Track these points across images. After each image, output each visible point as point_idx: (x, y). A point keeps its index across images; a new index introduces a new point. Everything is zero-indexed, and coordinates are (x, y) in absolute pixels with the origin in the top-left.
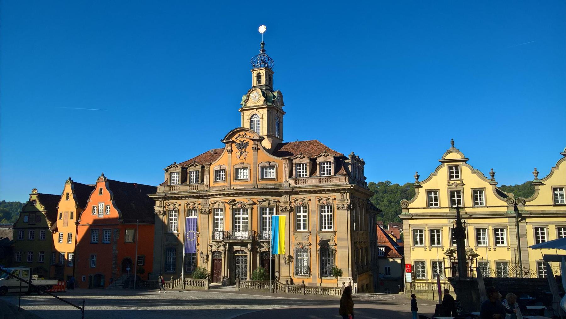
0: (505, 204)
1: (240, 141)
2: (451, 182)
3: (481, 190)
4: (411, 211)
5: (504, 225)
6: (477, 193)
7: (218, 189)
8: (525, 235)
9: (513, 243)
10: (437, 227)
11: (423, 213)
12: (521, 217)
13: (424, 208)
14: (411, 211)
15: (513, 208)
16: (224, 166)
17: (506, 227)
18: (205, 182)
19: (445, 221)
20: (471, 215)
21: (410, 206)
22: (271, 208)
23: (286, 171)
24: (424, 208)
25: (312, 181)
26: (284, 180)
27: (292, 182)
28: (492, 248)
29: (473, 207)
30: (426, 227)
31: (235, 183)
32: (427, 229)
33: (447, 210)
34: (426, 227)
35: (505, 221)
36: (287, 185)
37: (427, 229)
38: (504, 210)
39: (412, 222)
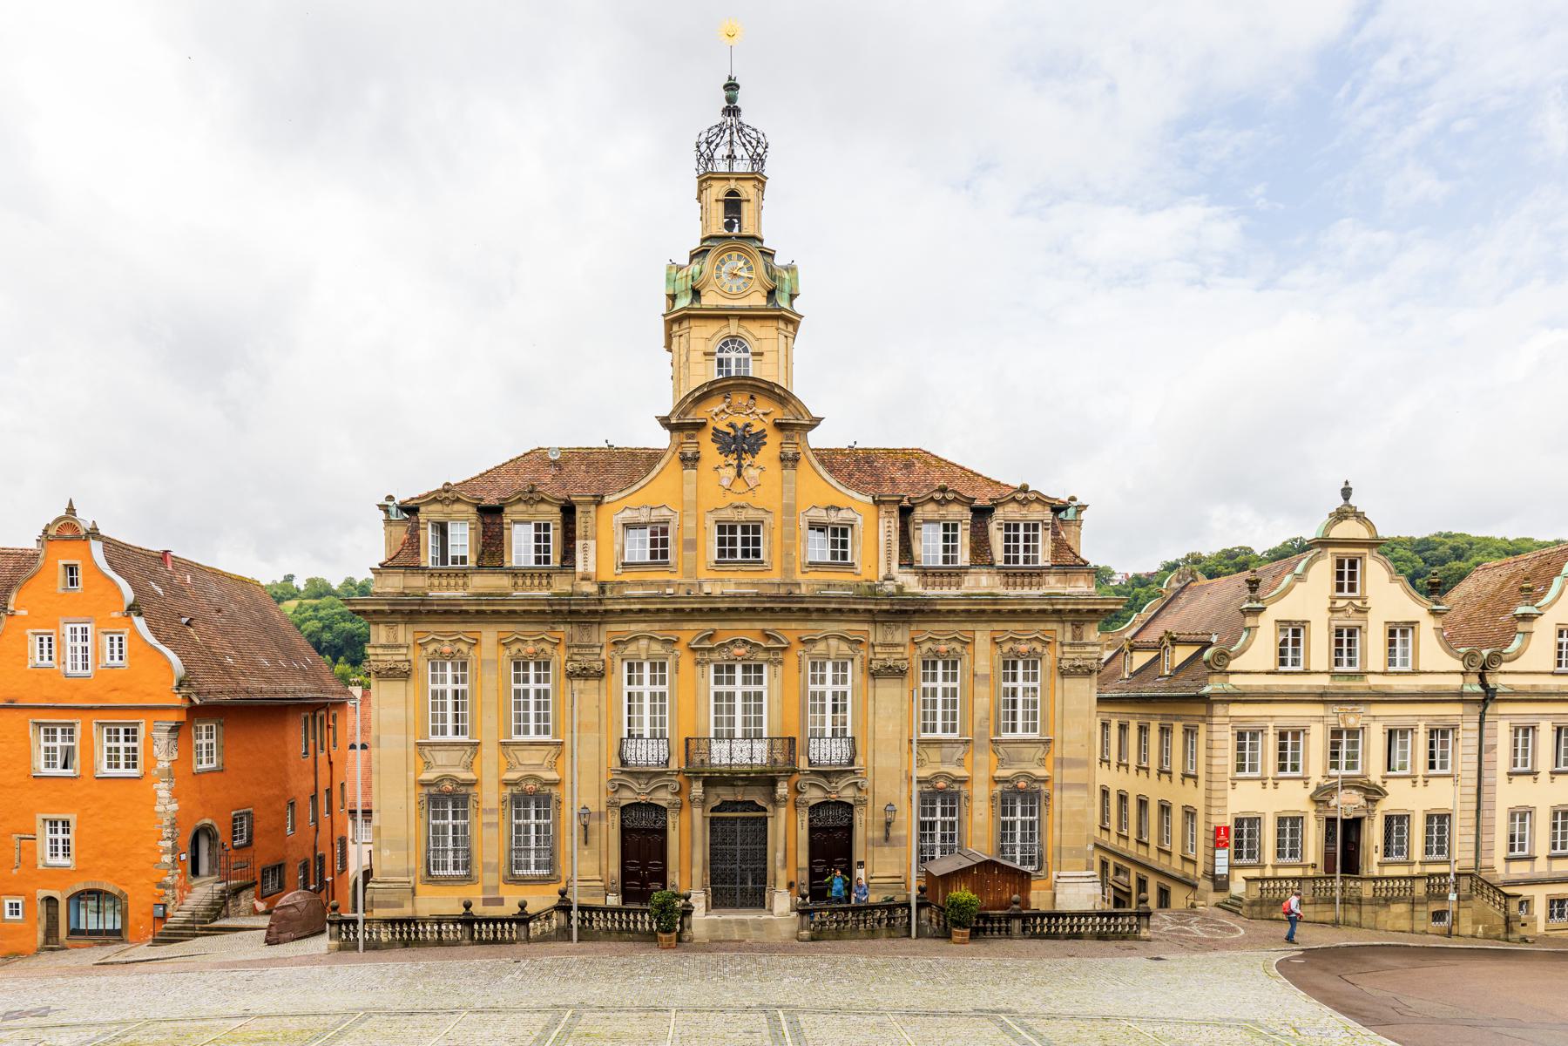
0: (1459, 666)
2: (1340, 604)
3: (1408, 627)
5: (1451, 721)
6: (1397, 632)
7: (639, 592)
8: (1494, 746)
9: (1465, 766)
10: (1299, 723)
11: (1266, 686)
12: (1489, 696)
14: (1235, 680)
15: (1476, 679)
17: (1454, 728)
18: (580, 568)
19: (1319, 710)
20: (1387, 694)
22: (840, 666)
24: (1268, 673)
26: (883, 572)
28: (1420, 780)
30: (1271, 725)
32: (1271, 731)
33: (1325, 681)
34: (1271, 725)
35: (1457, 709)
36: (890, 587)
37: (1271, 731)
38: (1455, 682)
39: (1236, 710)
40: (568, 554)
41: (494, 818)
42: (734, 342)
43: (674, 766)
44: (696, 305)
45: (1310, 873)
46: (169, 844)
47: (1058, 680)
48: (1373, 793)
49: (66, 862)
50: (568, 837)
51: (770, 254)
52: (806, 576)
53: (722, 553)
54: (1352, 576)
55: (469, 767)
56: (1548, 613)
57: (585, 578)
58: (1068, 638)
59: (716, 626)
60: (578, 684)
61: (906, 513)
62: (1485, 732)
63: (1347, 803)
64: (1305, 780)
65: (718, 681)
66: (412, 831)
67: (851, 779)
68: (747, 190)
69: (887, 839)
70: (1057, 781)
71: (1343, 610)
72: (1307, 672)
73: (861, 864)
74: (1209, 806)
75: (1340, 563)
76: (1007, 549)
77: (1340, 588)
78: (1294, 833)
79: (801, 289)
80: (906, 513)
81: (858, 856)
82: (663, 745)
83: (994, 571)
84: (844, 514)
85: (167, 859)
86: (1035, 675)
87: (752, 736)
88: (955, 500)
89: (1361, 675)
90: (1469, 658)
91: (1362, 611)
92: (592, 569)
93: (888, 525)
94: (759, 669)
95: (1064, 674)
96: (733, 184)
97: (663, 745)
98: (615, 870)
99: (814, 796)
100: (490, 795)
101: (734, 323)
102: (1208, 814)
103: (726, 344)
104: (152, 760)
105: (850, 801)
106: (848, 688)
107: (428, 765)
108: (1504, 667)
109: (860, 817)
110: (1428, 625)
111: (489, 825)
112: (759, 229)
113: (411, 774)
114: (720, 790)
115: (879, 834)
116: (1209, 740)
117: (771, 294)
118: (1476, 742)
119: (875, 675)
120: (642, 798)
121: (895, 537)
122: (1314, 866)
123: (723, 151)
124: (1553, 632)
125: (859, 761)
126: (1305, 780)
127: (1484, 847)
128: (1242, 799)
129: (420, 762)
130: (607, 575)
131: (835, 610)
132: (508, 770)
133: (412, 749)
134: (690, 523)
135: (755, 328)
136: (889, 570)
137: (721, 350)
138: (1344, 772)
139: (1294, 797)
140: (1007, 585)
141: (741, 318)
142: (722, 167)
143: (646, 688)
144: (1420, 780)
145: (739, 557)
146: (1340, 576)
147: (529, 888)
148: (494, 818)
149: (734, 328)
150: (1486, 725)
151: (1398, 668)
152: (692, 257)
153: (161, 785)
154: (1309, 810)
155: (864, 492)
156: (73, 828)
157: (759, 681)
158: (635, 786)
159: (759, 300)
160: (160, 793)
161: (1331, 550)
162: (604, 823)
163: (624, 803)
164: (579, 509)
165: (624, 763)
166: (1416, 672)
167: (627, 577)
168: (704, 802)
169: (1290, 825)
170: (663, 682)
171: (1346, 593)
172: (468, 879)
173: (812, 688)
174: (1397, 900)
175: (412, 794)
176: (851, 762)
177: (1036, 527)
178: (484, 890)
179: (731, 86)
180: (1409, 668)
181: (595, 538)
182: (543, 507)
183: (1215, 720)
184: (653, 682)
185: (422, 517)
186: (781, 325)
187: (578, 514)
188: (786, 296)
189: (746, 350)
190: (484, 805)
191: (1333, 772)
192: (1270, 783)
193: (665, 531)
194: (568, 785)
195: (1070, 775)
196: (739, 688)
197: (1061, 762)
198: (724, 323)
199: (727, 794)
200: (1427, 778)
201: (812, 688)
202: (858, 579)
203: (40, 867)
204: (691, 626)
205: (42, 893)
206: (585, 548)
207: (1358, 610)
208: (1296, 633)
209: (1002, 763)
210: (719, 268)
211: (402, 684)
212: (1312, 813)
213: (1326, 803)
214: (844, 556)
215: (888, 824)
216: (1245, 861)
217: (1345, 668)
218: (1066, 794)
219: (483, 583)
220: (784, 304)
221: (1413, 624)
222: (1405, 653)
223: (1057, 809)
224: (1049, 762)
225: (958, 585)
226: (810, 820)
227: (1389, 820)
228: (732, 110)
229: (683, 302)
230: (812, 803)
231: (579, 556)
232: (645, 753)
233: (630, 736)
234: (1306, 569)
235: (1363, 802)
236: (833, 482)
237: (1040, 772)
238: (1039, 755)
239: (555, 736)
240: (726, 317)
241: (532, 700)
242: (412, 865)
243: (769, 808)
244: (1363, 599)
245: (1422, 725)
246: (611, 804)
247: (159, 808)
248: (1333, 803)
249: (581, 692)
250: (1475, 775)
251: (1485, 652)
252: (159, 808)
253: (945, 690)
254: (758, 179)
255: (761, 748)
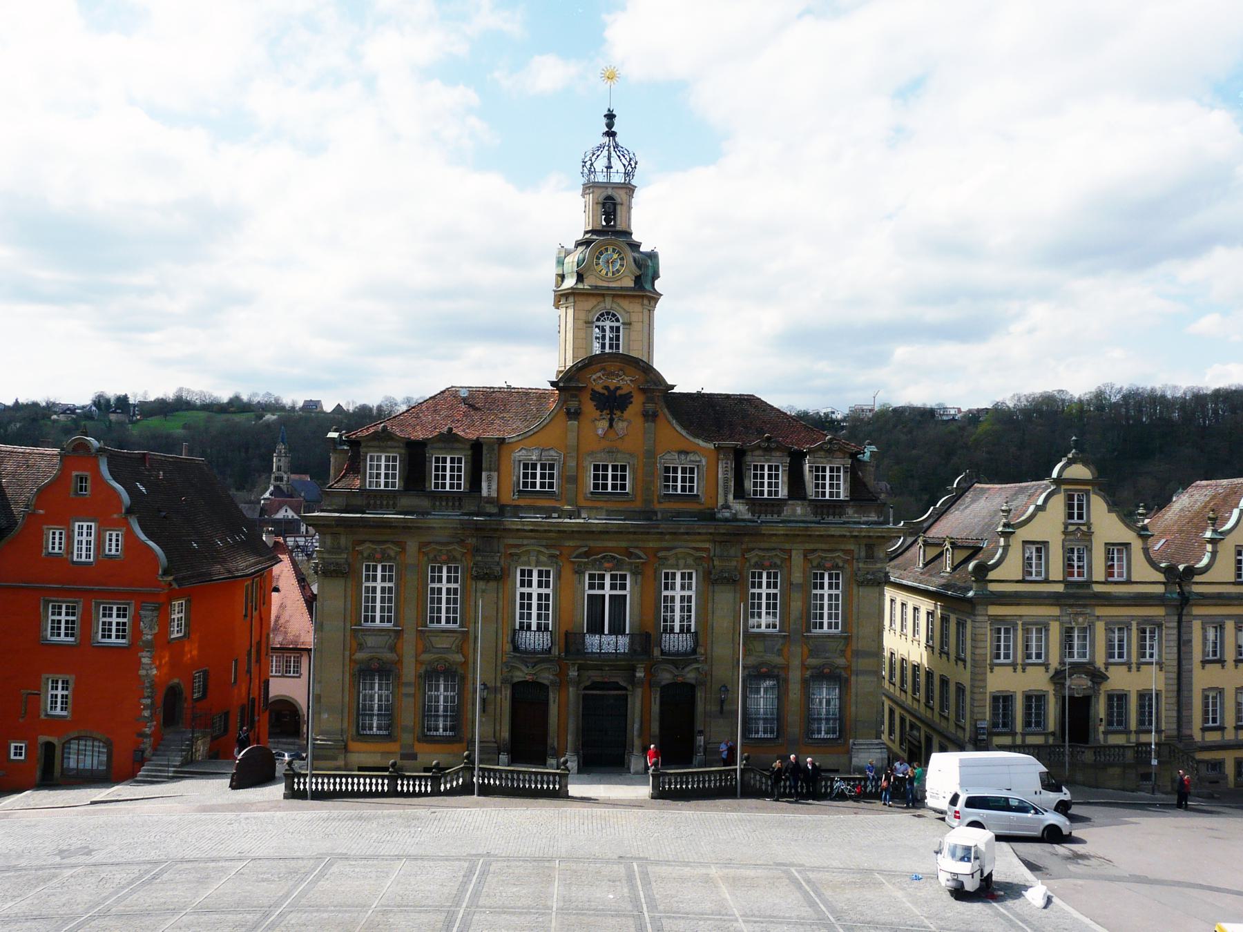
0: (1161, 577)
1: (606, 388)
2: (1071, 528)
4: (993, 587)
8: (1190, 641)
9: (1169, 657)
13: (1018, 582)
16: (552, 453)
17: (1160, 626)
18: (485, 493)
19: (1055, 611)
21: (992, 575)
23: (726, 480)
24: (1018, 582)
25: (794, 511)
26: (721, 502)
27: (740, 508)
28: (1134, 666)
29: (1106, 583)
30: (1020, 623)
31: (590, 504)
32: (1020, 627)
33: (1060, 588)
34: (1020, 623)
35: (1158, 612)
37: (1020, 627)
38: (1160, 589)
39: (994, 610)
40: (475, 483)
41: (411, 690)
42: (608, 313)
43: (555, 651)
44: (580, 286)
45: (1051, 741)
46: (148, 701)
47: (855, 587)
48: (1098, 677)
49: (64, 713)
50: (470, 707)
51: (635, 246)
52: (662, 506)
53: (596, 486)
54: (1080, 507)
55: (393, 649)
56: (1228, 538)
57: (489, 500)
58: (863, 554)
59: (591, 544)
60: (481, 585)
61: (739, 456)
62: (1183, 630)
63: (1078, 684)
64: (1046, 666)
65: (592, 587)
66: (347, 699)
67: (695, 666)
68: (620, 196)
69: (721, 711)
70: (854, 668)
71: (1073, 533)
72: (1047, 581)
73: (701, 732)
74: (973, 686)
75: (1071, 498)
76: (817, 486)
77: (1071, 516)
78: (1038, 707)
79: (661, 273)
80: (739, 456)
81: (699, 726)
82: (547, 636)
83: (806, 503)
84: (692, 457)
85: (146, 713)
86: (837, 584)
87: (617, 629)
88: (777, 449)
89: (1089, 583)
90: (1170, 571)
91: (1089, 535)
92: (494, 495)
93: (724, 471)
94: (623, 577)
95: (861, 584)
96: (610, 192)
97: (547, 636)
98: (506, 734)
99: (666, 677)
100: (409, 671)
101: (608, 301)
102: (972, 692)
103: (602, 315)
104: (137, 633)
105: (693, 682)
106: (692, 593)
107: (361, 647)
108: (1197, 579)
109: (699, 694)
110: (1137, 545)
111: (407, 695)
112: (629, 226)
113: (347, 653)
114: (591, 673)
115: (715, 708)
116: (974, 635)
117: (638, 279)
118: (1175, 637)
119: (714, 582)
120: (528, 678)
121: (731, 475)
122: (1053, 734)
123: (600, 164)
124: (1233, 551)
125: (701, 650)
126: (1046, 666)
127: (1184, 719)
128: (1000, 680)
129: (355, 645)
130: (509, 498)
131: (683, 534)
132: (424, 652)
133: (348, 633)
134: (572, 463)
135: (625, 304)
136: (726, 500)
137: (598, 320)
138: (1076, 659)
139: (1038, 680)
140: (815, 514)
141: (614, 296)
142: (601, 178)
143: (535, 590)
144: (1134, 666)
145: (610, 490)
146: (1071, 507)
147: (438, 747)
148: (411, 690)
149: (608, 304)
150: (1184, 624)
151: (1116, 578)
152: (576, 247)
153: (144, 654)
154: (1049, 688)
155: (706, 440)
156: (71, 686)
157: (623, 587)
158: (524, 668)
159: (629, 283)
160: (145, 660)
161: (1063, 487)
162: (499, 696)
163: (516, 680)
164: (485, 448)
165: (516, 648)
166: (1129, 582)
167: (522, 503)
168: (579, 683)
169: (1034, 701)
170: (547, 586)
171: (1076, 520)
172: (389, 738)
173: (665, 593)
174: (1112, 765)
175: (347, 668)
176: (694, 651)
177: (838, 470)
178: (401, 747)
179: (610, 117)
180: (1124, 578)
181: (498, 470)
182: (456, 445)
183: (979, 618)
184: (540, 585)
185: (362, 450)
186: (646, 302)
187: (485, 452)
188: (650, 278)
189: (617, 320)
190: (405, 680)
191: (1068, 660)
192: (1019, 667)
193: (552, 467)
194: (471, 664)
195: (863, 664)
196: (607, 591)
197: (857, 654)
198: (601, 299)
199: (596, 676)
200: (1139, 665)
201: (665, 593)
202: (700, 507)
203: (42, 717)
204: (571, 543)
205: (42, 739)
206: (489, 479)
207: (1084, 533)
208: (1039, 550)
209: (813, 653)
210: (598, 258)
211: (342, 582)
212: (1051, 692)
213: (1063, 685)
214: (691, 488)
215: (722, 702)
216: (1001, 729)
217: (1076, 578)
218: (861, 678)
219: (404, 502)
220: (648, 287)
221: (1127, 545)
222: (1121, 567)
223: (853, 690)
224: (849, 653)
225: (779, 514)
226: (661, 697)
227: (1110, 697)
228: (611, 134)
229: (570, 282)
230: (663, 683)
231: (484, 485)
232: (534, 640)
233: (521, 628)
234: (1046, 500)
235: (1090, 683)
236: (684, 433)
237: (841, 661)
238: (841, 647)
239: (462, 626)
240: (603, 295)
241: (444, 596)
242: (345, 725)
243: (630, 687)
244: (1089, 525)
245: (1134, 624)
246: (504, 681)
247: (142, 672)
248: (1068, 683)
249: (483, 591)
250: (1175, 663)
251: (1181, 567)
252: (142, 672)
253: (768, 595)
254: (629, 189)
255: (627, 640)
